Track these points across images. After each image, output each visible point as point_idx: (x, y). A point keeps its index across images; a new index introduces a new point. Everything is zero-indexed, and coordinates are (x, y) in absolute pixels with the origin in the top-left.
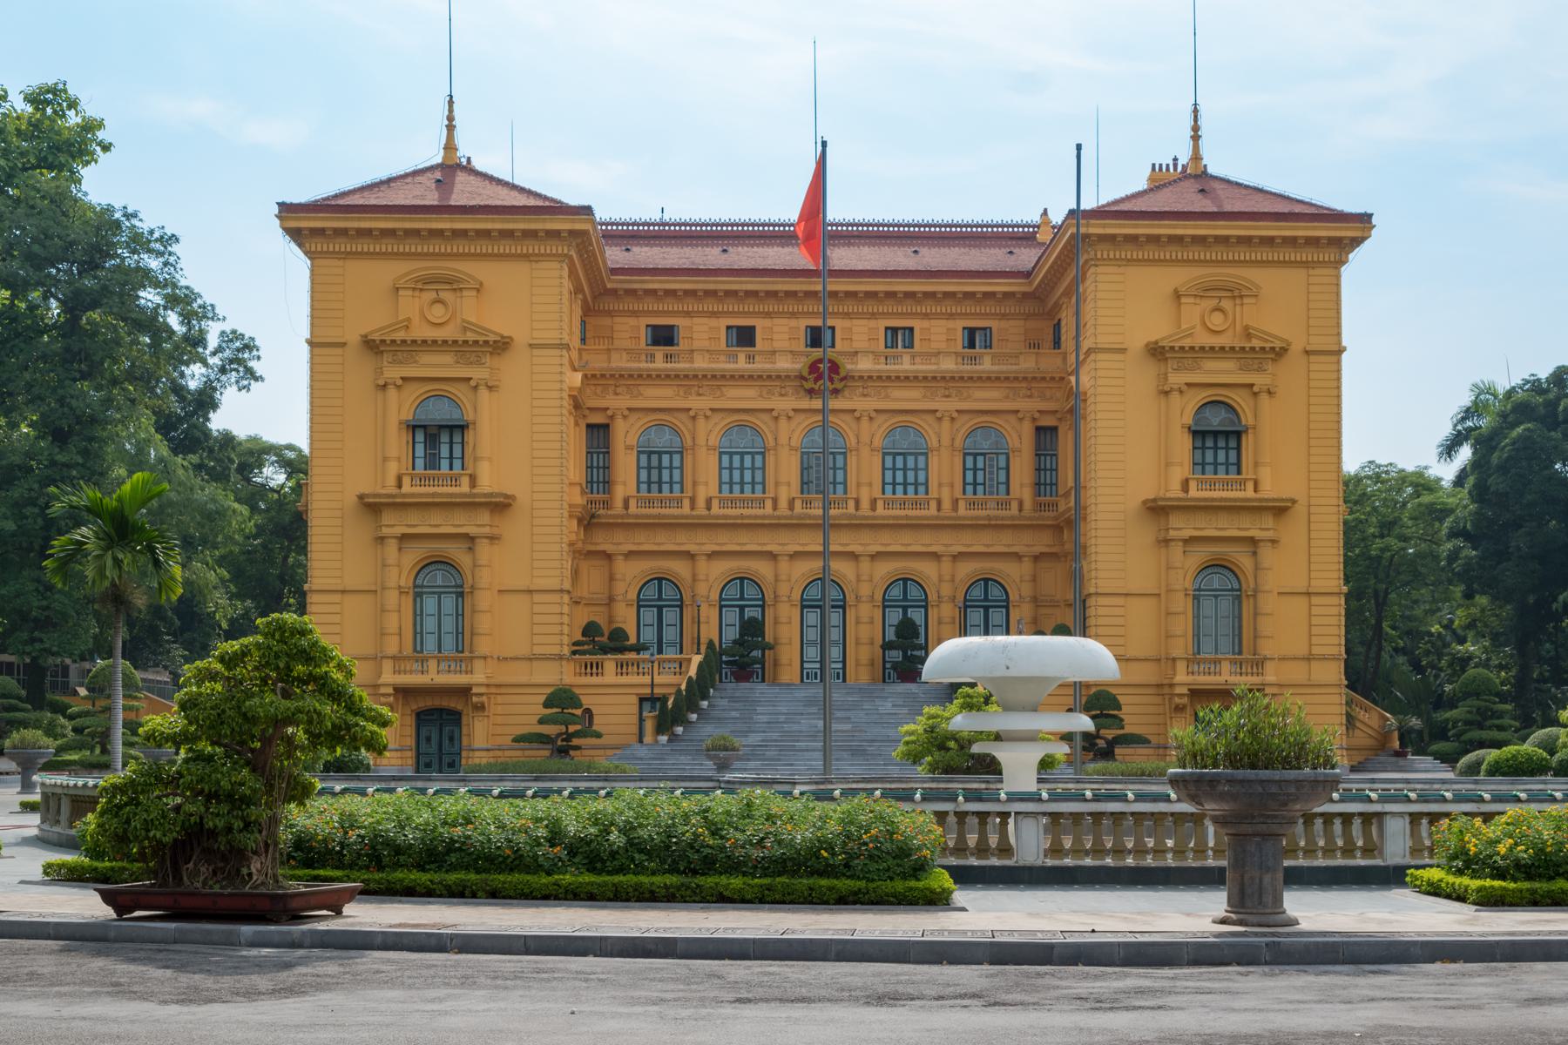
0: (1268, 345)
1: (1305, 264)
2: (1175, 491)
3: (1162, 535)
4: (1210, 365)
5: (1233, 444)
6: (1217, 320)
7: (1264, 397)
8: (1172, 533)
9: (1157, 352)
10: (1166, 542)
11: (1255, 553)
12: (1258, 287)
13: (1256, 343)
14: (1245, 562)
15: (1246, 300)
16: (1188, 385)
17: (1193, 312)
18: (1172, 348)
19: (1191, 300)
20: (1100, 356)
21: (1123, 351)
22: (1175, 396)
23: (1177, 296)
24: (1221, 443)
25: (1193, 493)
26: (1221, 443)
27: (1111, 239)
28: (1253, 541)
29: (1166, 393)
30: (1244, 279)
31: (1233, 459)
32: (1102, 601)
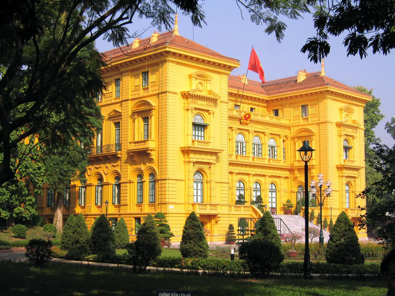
0: (215, 98)
1: (219, 73)
2: (190, 144)
3: (187, 160)
4: (200, 102)
5: (203, 130)
6: (200, 86)
7: (212, 115)
8: (191, 160)
9: (186, 96)
10: (189, 162)
11: (210, 167)
12: (212, 79)
13: (212, 96)
14: (208, 171)
15: (208, 82)
16: (196, 109)
17: (195, 83)
18: (192, 94)
19: (195, 79)
20: (170, 94)
21: (176, 93)
22: (190, 112)
23: (190, 76)
24: (200, 129)
25: (196, 145)
26: (200, 129)
27: (174, 54)
28: (209, 164)
29: (188, 110)
30: (209, 75)
31: (203, 135)
32: (170, 182)
